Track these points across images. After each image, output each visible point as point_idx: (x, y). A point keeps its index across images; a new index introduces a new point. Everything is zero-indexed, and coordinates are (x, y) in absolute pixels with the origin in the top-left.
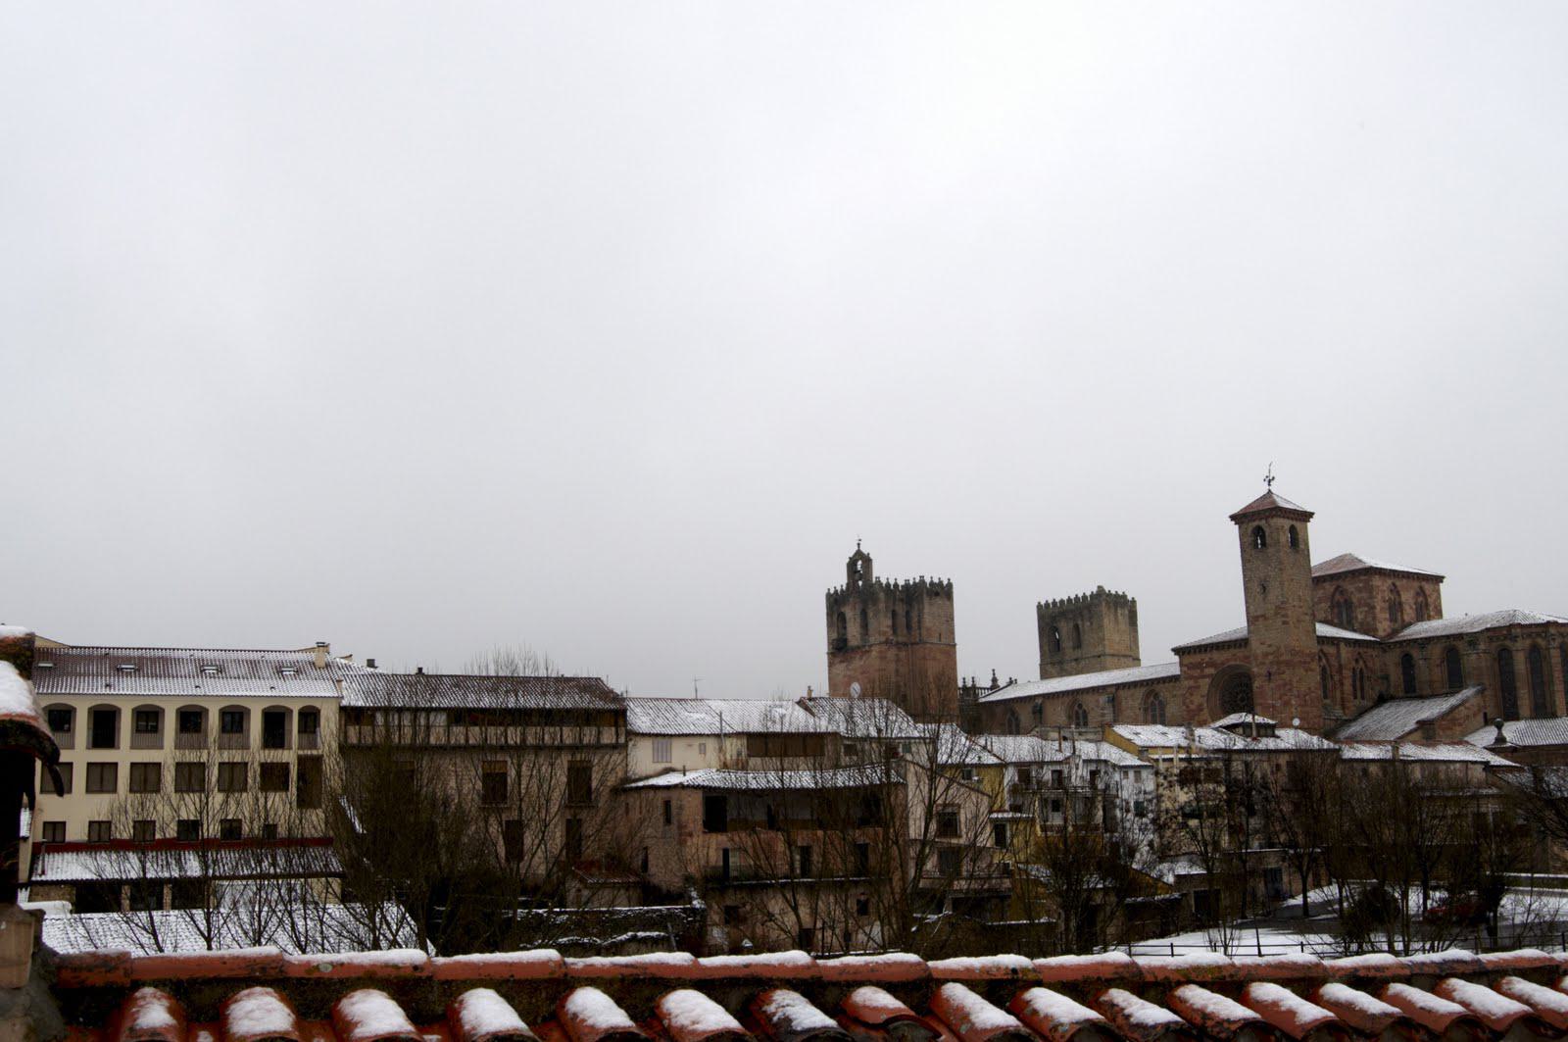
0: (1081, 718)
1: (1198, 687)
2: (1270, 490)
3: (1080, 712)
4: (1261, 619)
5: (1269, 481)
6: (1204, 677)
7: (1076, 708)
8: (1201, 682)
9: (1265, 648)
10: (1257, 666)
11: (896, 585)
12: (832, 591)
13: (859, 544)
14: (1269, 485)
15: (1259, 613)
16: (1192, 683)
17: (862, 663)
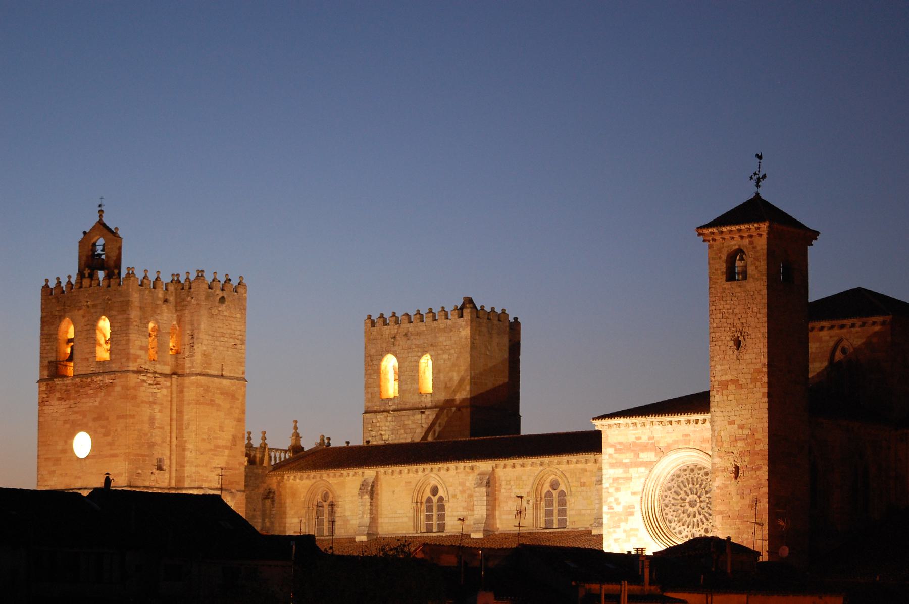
0: (435, 509)
2: (757, 194)
3: (435, 499)
4: (732, 387)
5: (758, 181)
8: (633, 471)
12: (52, 284)
13: (101, 212)
14: (758, 186)
15: (729, 378)
17: (97, 403)
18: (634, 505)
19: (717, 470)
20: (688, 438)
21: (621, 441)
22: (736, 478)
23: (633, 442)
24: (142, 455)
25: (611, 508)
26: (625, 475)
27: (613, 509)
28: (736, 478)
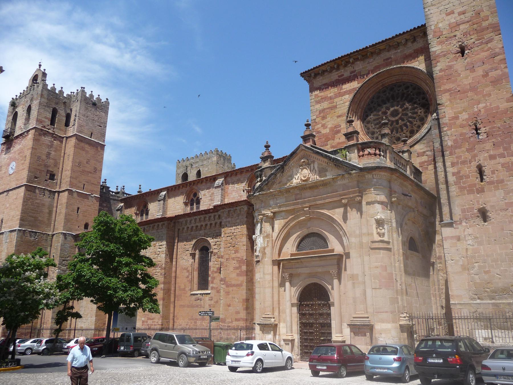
1: (335, 107)
6: (341, 95)
7: (192, 196)
9: (453, 19)
10: (441, 43)
11: (61, 92)
16: (325, 105)
18: (340, 125)
19: (437, 56)
20: (390, 60)
21: (325, 83)
22: (463, 56)
23: (336, 79)
24: (39, 170)
25: (319, 132)
26: (330, 105)
27: (321, 132)
28: (463, 56)
